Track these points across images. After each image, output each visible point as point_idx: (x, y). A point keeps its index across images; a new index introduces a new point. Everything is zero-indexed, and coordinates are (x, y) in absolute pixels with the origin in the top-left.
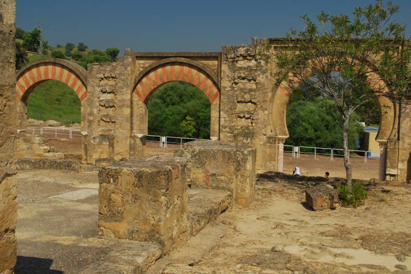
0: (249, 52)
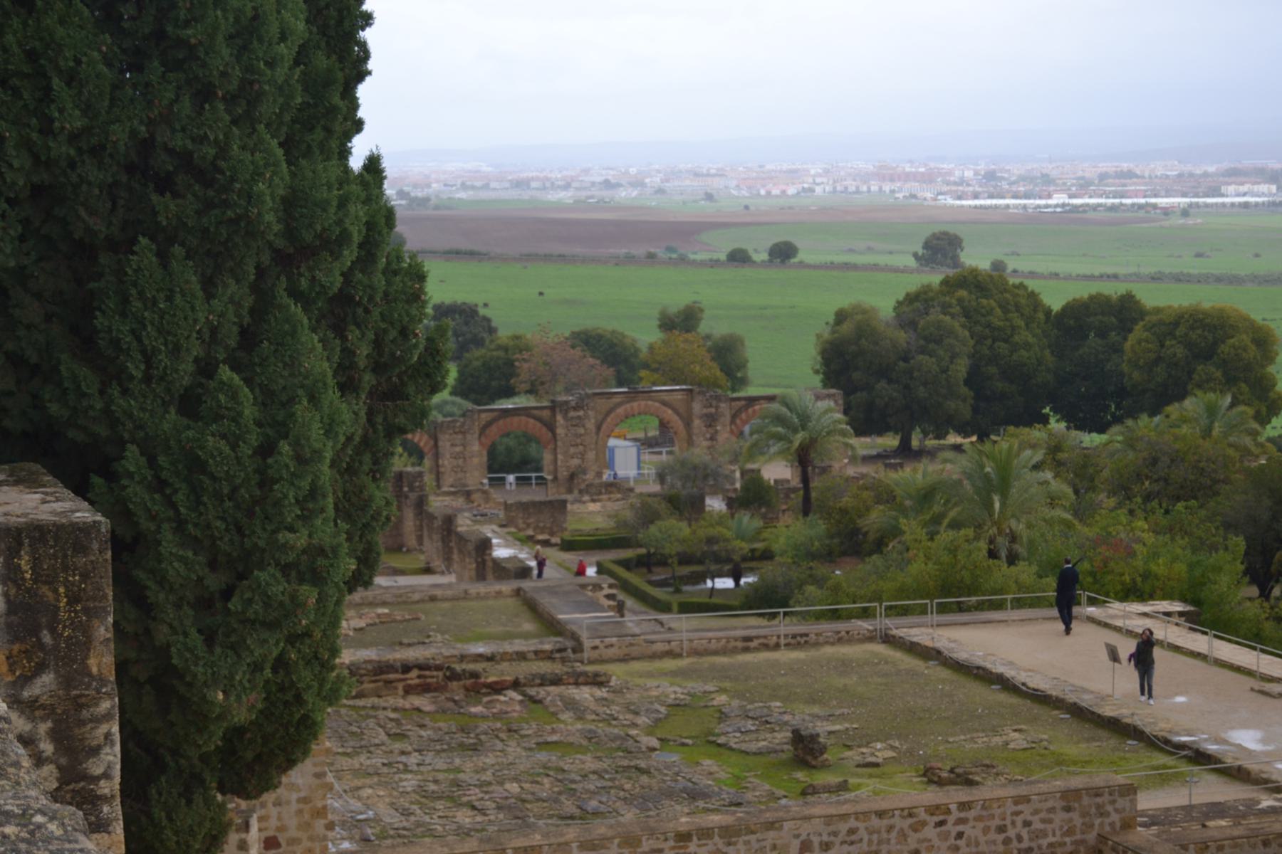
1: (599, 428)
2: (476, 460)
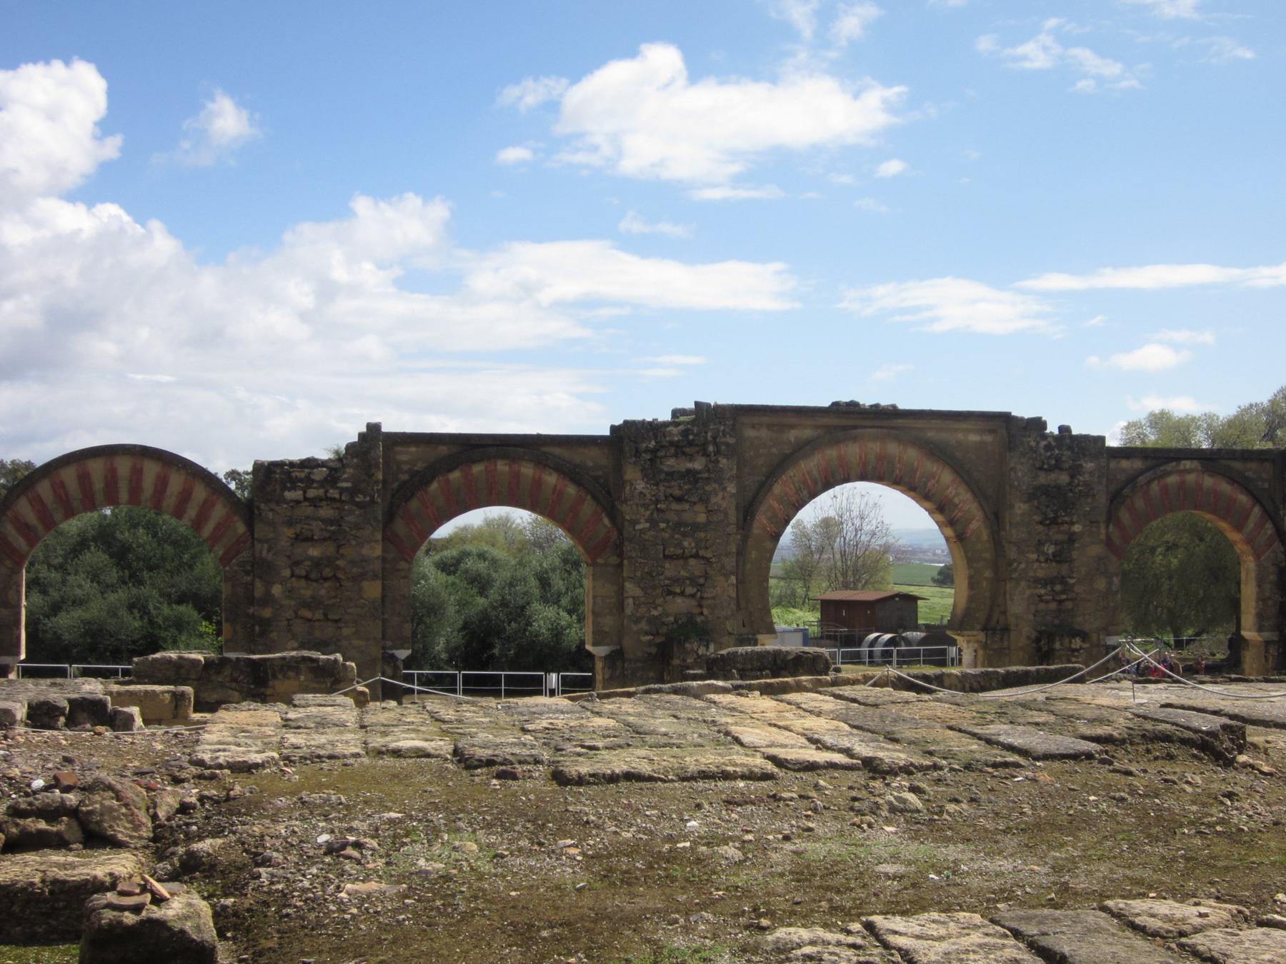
0: (691, 437)
1: (747, 512)
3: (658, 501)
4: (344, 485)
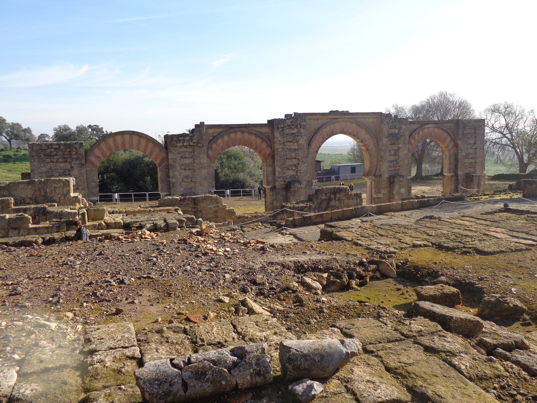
2: (204, 172)
3: (284, 143)
4: (195, 141)
